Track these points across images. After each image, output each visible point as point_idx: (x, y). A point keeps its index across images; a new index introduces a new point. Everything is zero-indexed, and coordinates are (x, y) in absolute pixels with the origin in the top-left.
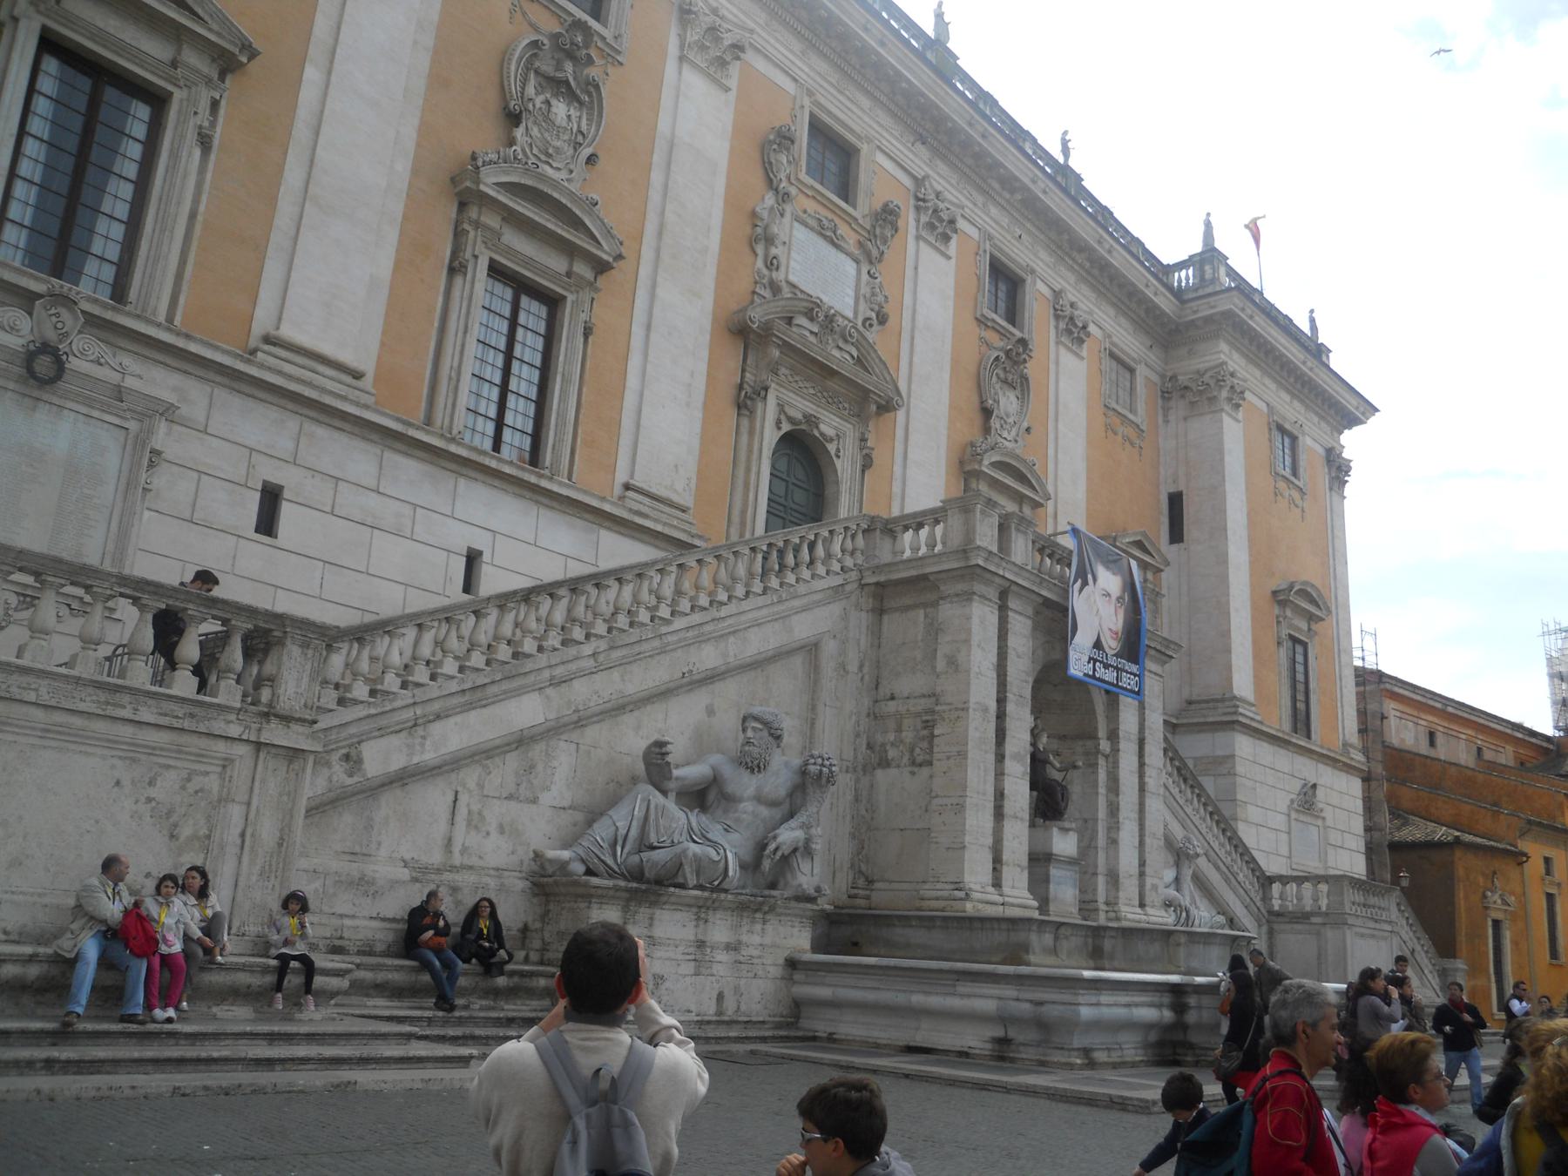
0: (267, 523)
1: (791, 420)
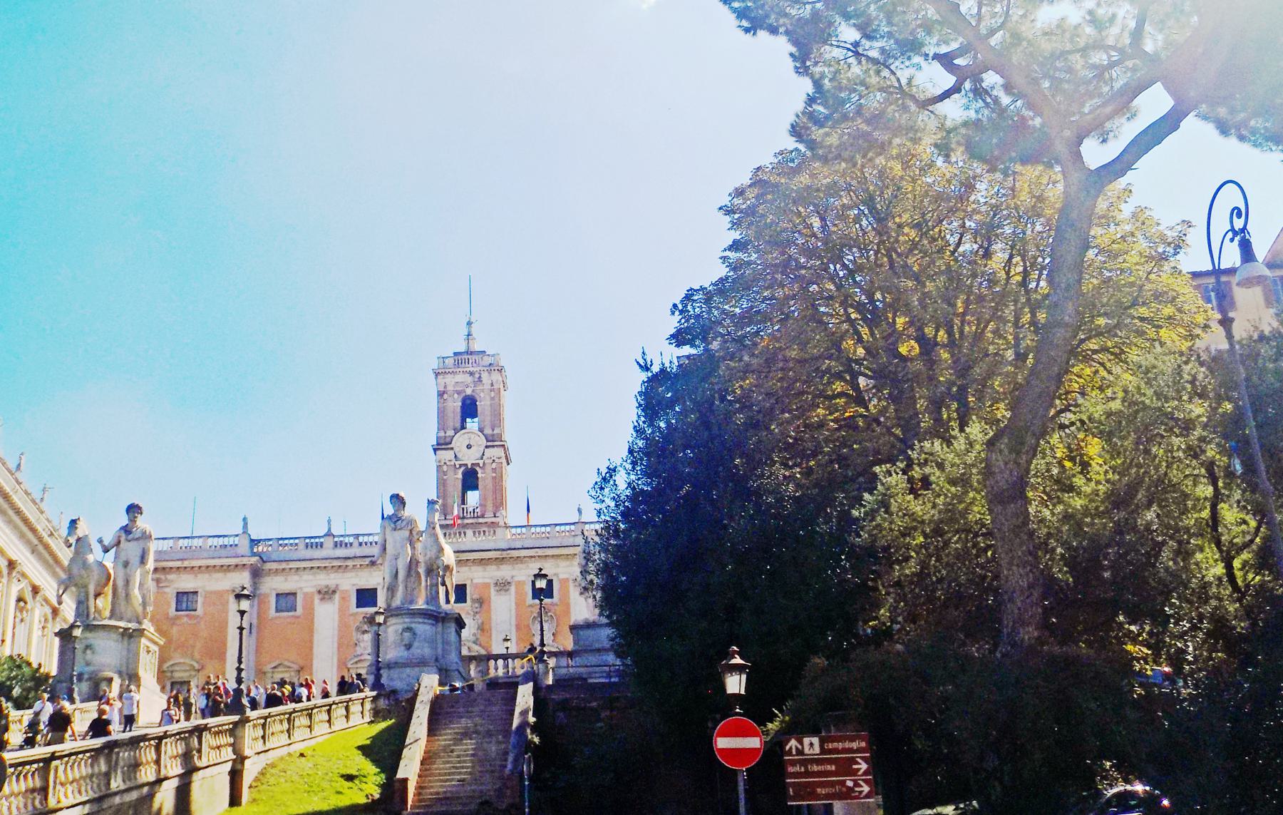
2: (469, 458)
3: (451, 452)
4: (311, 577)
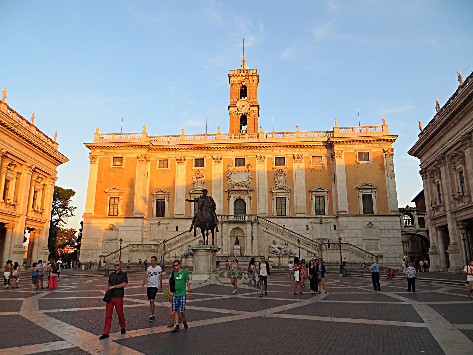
0: (177, 230)
1: (236, 198)
2: (244, 111)
3: (236, 108)
4: (174, 153)
